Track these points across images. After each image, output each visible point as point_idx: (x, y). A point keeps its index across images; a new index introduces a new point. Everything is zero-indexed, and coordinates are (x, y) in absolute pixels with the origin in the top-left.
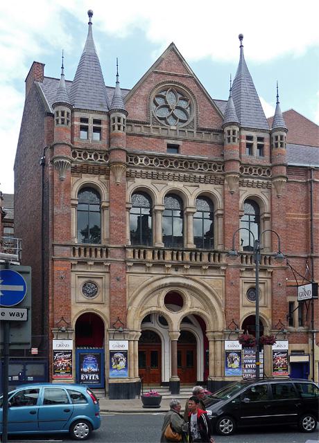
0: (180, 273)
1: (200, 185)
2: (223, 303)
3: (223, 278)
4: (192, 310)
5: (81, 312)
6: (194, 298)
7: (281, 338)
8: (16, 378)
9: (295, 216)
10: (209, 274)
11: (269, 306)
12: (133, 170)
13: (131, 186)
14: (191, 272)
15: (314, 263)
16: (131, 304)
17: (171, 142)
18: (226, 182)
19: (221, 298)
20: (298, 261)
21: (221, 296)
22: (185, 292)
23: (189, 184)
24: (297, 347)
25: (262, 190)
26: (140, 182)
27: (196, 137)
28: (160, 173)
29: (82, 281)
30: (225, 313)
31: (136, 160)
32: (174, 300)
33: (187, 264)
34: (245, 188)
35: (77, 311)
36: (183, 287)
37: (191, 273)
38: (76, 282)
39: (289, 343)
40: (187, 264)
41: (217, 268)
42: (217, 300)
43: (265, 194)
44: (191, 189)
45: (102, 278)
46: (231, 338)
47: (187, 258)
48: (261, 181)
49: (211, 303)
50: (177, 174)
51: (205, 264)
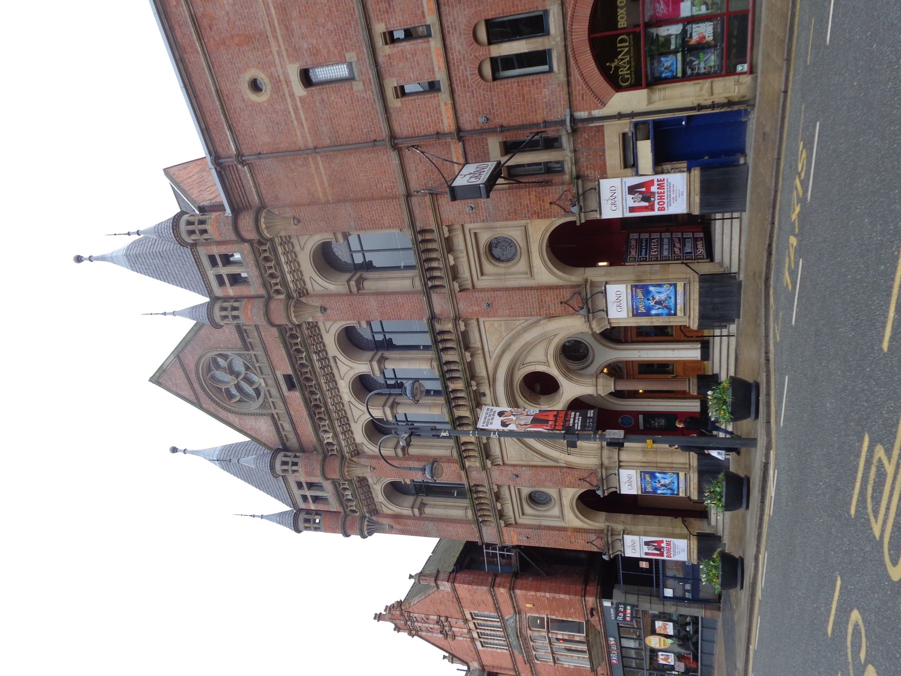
0: (485, 389)
1: (330, 355)
4: (552, 362)
5: (577, 517)
6: (530, 359)
7: (592, 197)
8: (688, 587)
9: (322, 183)
10: (478, 345)
11: (523, 222)
12: (346, 450)
13: (370, 448)
14: (481, 371)
15: (405, 133)
17: (284, 388)
19: (521, 323)
20: (410, 166)
21: (518, 323)
23: (335, 371)
25: (297, 249)
26: (359, 436)
27: (260, 352)
28: (335, 415)
29: (528, 510)
30: (551, 317)
31: (329, 444)
33: (468, 385)
35: (573, 520)
37: (484, 374)
38: (531, 516)
39: (604, 175)
41: (465, 335)
42: (526, 329)
43: (302, 242)
44: (343, 369)
45: (519, 489)
46: (601, 306)
47: (460, 385)
50: (328, 394)
51: (462, 357)
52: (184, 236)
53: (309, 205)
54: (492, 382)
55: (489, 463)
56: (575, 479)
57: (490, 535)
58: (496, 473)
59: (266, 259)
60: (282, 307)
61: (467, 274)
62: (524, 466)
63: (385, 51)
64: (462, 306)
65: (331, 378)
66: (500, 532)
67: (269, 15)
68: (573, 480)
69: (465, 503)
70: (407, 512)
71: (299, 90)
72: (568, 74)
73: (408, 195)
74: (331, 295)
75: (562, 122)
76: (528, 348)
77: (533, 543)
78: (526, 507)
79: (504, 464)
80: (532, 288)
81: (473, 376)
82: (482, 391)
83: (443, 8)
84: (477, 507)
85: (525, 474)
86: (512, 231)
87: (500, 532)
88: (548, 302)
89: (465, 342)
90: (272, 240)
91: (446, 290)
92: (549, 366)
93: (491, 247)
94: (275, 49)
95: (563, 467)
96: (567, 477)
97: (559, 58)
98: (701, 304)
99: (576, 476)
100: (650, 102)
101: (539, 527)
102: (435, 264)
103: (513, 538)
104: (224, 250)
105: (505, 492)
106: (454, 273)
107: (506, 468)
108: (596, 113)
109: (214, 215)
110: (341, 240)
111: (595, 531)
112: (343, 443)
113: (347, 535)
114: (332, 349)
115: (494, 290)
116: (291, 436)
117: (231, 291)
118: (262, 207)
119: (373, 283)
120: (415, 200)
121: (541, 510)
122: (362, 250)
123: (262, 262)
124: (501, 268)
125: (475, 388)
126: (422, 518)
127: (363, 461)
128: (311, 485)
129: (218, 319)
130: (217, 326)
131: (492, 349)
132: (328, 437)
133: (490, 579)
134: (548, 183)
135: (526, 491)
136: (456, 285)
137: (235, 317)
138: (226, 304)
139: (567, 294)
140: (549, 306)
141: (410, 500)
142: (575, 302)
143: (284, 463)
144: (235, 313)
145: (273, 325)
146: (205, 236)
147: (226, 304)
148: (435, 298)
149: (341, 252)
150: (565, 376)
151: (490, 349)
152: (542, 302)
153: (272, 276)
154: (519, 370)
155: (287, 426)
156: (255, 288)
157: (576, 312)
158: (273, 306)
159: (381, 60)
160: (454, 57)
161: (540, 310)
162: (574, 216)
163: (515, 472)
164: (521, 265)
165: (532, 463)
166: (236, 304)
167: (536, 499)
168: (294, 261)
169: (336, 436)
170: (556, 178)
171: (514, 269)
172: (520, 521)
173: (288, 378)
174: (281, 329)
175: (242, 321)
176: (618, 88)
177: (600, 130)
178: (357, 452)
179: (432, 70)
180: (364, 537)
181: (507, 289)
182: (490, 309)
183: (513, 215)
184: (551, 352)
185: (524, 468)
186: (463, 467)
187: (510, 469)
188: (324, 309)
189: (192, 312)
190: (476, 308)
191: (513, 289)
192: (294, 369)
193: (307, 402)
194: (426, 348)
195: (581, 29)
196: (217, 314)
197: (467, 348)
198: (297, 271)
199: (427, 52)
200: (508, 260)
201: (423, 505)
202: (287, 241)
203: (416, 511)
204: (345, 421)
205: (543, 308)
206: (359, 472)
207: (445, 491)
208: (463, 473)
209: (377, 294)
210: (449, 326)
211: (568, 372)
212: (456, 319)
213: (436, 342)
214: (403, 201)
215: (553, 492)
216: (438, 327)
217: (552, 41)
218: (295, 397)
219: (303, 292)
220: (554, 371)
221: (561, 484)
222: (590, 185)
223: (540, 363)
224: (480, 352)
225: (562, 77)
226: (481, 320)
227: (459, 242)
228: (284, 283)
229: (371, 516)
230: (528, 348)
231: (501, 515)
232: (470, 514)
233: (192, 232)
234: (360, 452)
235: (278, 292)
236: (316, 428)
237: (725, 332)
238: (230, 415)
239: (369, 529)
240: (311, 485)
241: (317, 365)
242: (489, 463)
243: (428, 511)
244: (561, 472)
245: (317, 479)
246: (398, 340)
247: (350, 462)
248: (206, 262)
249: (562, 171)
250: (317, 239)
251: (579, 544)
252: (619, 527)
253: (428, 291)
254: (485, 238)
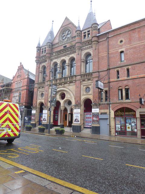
0: (62, 86)
8: (27, 121)
9: (102, 55)
10: (70, 85)
12: (52, 58)
13: (52, 63)
15: (110, 72)
17: (64, 45)
19: (74, 93)
20: (104, 73)
22: (65, 92)
23: (67, 56)
24: (103, 111)
25: (90, 49)
26: (54, 61)
29: (40, 93)
30: (75, 99)
32: (63, 96)
33: (63, 83)
34: (84, 51)
35: (39, 101)
36: (64, 91)
37: (65, 86)
40: (63, 83)
41: (72, 82)
42: (73, 94)
44: (67, 58)
47: (63, 81)
48: (88, 46)
51: (68, 82)
52: (94, 25)
53: (98, 52)
54: (64, 87)
55: (49, 86)
57: (36, 86)
58: (47, 87)
59: (88, 43)
60: (79, 46)
61: (83, 83)
63: (126, 68)
64: (78, 82)
65: (65, 55)
66: (36, 88)
67: (134, 45)
69: (42, 81)
70: (40, 70)
71: (120, 50)
72: (118, 103)
73: (99, 72)
74: (81, 56)
75: (110, 102)
76: (70, 94)
77: (34, 94)
78: (41, 92)
80: (80, 95)
81: (65, 83)
83: (132, 80)
84: (41, 83)
86: (91, 92)
87: (36, 88)
89: (71, 82)
90: (92, 44)
91: (81, 79)
93: (89, 88)
94: (128, 46)
97: (121, 102)
98: (76, 126)
100: (112, 118)
101: (37, 95)
102: (86, 77)
103: (35, 90)
104: (91, 34)
105: (43, 89)
106: (84, 80)
108: (111, 108)
109: (97, 32)
110: (91, 58)
111: (36, 105)
112: (53, 57)
113: (36, 57)
114: (71, 56)
115: (80, 88)
116: (55, 47)
117: (83, 35)
118: (98, 42)
119: (83, 64)
120: (98, 73)
121: (40, 95)
122: (90, 62)
123: (88, 42)
124: (84, 89)
126: (39, 73)
128: (45, 50)
129: (77, 32)
130: (76, 32)
132: (54, 54)
133: (28, 85)
134: (99, 99)
135: (44, 93)
136: (81, 81)
137: (77, 36)
138: (80, 34)
139: (79, 102)
141: (43, 70)
142: (77, 103)
143: (49, 45)
144: (78, 36)
145: (76, 44)
146: (93, 30)
147: (80, 34)
148: (79, 77)
149: (90, 58)
150: (65, 101)
153: (85, 44)
155: (57, 46)
156: (83, 40)
157: (76, 103)
158: (79, 44)
159: (124, 67)
160: (123, 82)
162: (93, 104)
164: (85, 93)
166: (80, 36)
167: (42, 94)
168: (88, 48)
169: (54, 56)
170: (100, 100)
171: (84, 92)
172: (38, 91)
173: (66, 46)
174: (75, 45)
175: (77, 37)
176: (115, 112)
177: (108, 109)
178: (51, 60)
179: (121, 77)
180: (36, 61)
181: (80, 91)
182: (77, 87)
183: (94, 92)
184: (69, 98)
186: (48, 81)
188: (78, 54)
189: (79, 27)
190: (77, 84)
191: (80, 92)
192: (68, 48)
193: (61, 50)
194: (71, 74)
195: (126, 106)
196: (78, 32)
197: (70, 82)
198: (86, 49)
199: (124, 76)
200: (86, 91)
201: (41, 73)
202: (92, 47)
203: (40, 71)
204: (57, 58)
206: (48, 60)
207: (44, 78)
208: (47, 81)
209: (81, 65)
210: (74, 79)
211: (65, 101)
212: (75, 81)
213: (71, 77)
214: (98, 71)
215: (43, 98)
216: (74, 77)
217: (125, 100)
218: (62, 48)
219: (82, 50)
220: (65, 99)
221: (45, 100)
222: (98, 107)
223: (67, 96)
225: (118, 102)
226: (75, 85)
227: (90, 82)
228: (83, 47)
230: (70, 94)
231: (39, 88)
232: (40, 82)
233: (94, 27)
235: (82, 45)
236: (56, 52)
237: (71, 130)
240: (45, 50)
241: (68, 53)
242: (49, 86)
243: (40, 74)
245: (46, 52)
246: (72, 69)
248: (88, 30)
249: (101, 101)
250: (92, 53)
251: (34, 102)
252: (37, 110)
253: (81, 75)
254: (90, 87)
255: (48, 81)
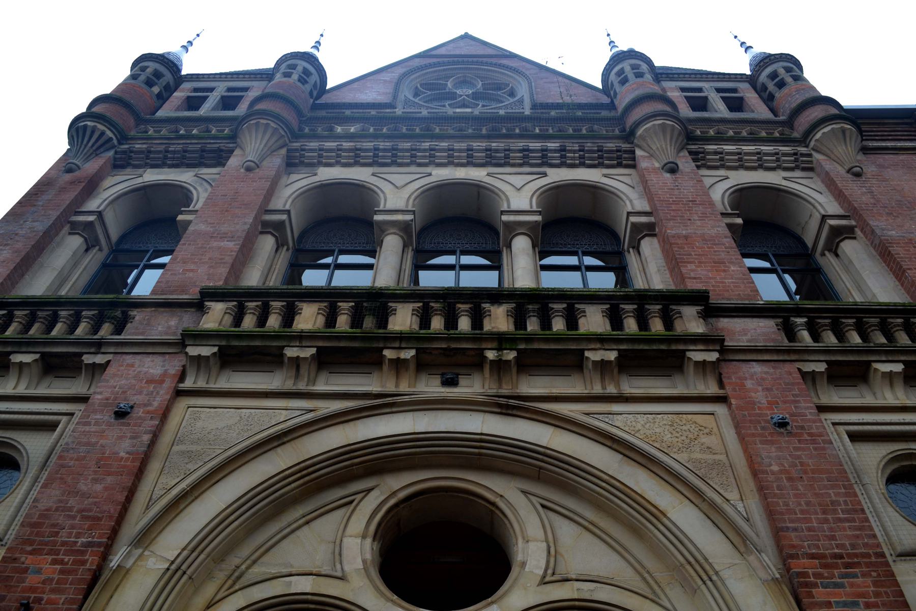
2: (761, 530)
3: (720, 410)
6: (566, 531)
16: (145, 538)
18: (639, 152)
49: (679, 538)
56: (32, 589)
62: (153, 443)
68: (31, 579)
79: (180, 393)
82: (463, 381)
85: (120, 438)
88: (852, 585)
92: (543, 582)
95: (105, 557)
96: (55, 562)
99: (45, 597)
107: (163, 394)
125: (491, 355)
127: (277, 161)
131: (619, 421)
140: (836, 585)
151: (619, 417)
152: (848, 566)
154: (524, 492)
161: (813, 556)
163: (139, 412)
165: (154, 467)
185: (146, 438)
187: (157, 403)
205: (825, 566)
223: (553, 554)
224: (611, 390)
229: (116, 153)
234: (293, 169)
238: (404, 70)
239: (93, 132)
244: (90, 544)
247: (281, 142)
255: (210, 295)
